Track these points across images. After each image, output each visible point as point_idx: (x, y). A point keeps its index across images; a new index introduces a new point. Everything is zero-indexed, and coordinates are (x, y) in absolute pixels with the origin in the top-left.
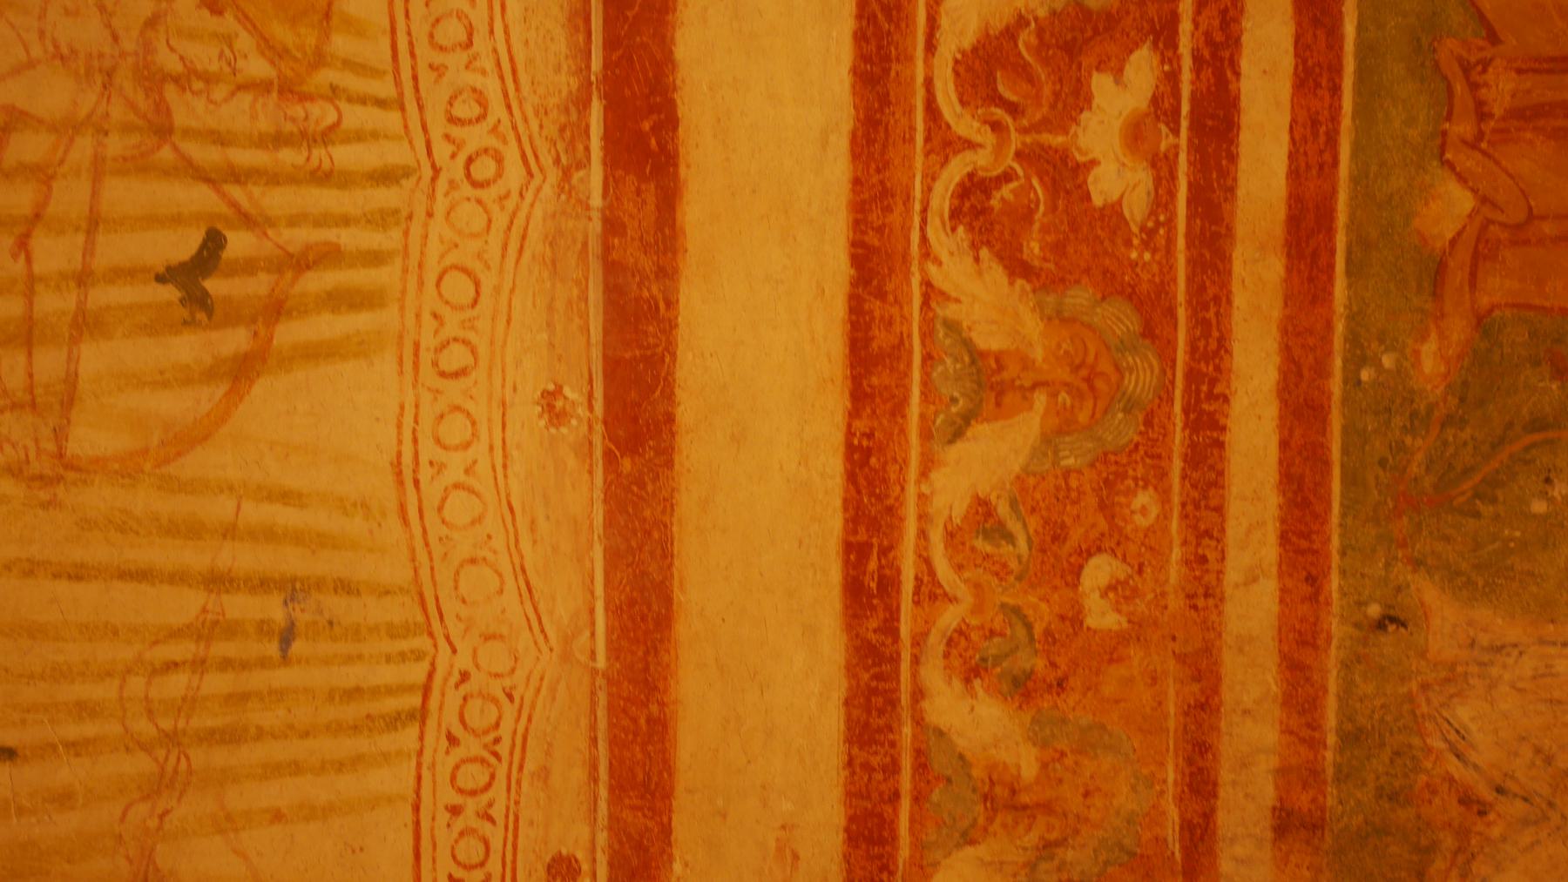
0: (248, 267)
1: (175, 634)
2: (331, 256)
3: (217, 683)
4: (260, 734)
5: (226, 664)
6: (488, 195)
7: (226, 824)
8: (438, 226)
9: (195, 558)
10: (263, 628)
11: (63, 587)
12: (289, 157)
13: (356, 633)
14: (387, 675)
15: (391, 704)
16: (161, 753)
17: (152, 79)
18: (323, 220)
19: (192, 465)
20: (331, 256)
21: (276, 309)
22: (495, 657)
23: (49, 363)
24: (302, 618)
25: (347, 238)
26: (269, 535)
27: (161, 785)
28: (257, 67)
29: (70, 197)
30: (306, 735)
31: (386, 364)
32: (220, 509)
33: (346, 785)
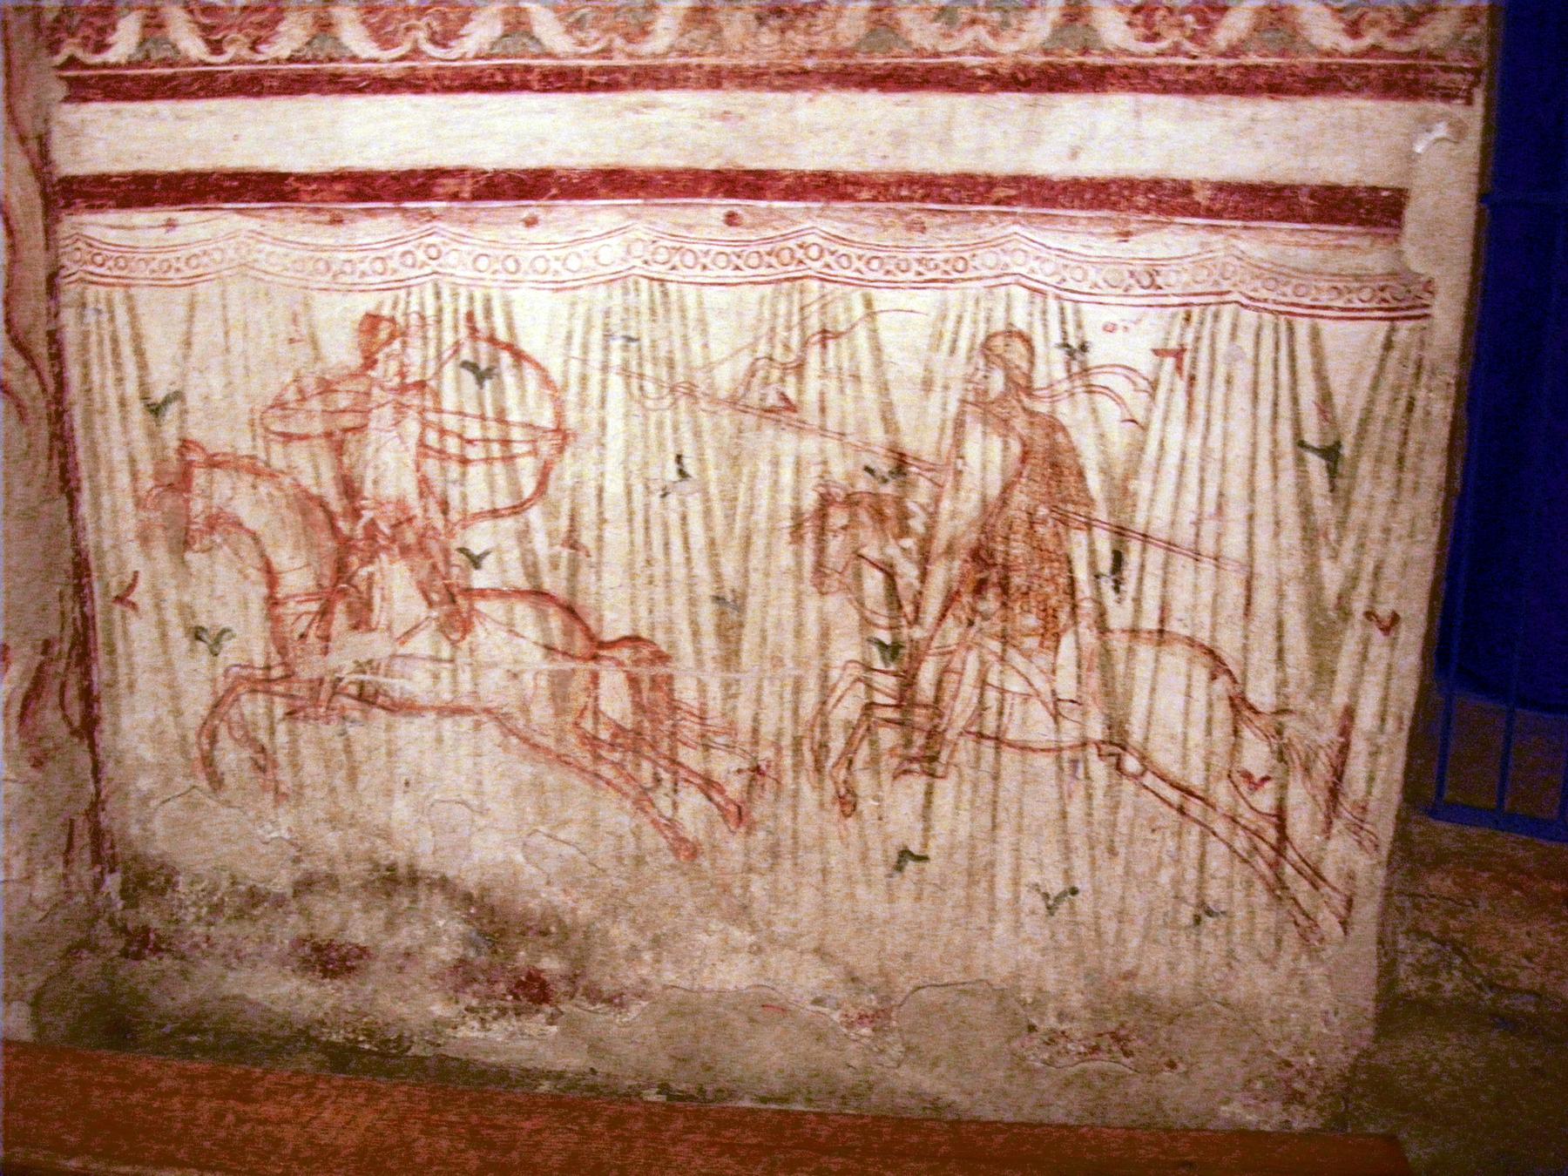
0: (475, 351)
1: (628, 385)
2: (470, 317)
5: (640, 365)
6: (444, 249)
7: (709, 367)
8: (457, 272)
12: (431, 333)
14: (645, 296)
15: (658, 294)
17: (403, 388)
18: (456, 321)
19: (556, 375)
20: (470, 317)
21: (492, 340)
22: (638, 249)
23: (516, 434)
25: (463, 310)
26: (585, 347)
28: (397, 345)
29: (451, 422)
31: (513, 294)
32: (575, 367)
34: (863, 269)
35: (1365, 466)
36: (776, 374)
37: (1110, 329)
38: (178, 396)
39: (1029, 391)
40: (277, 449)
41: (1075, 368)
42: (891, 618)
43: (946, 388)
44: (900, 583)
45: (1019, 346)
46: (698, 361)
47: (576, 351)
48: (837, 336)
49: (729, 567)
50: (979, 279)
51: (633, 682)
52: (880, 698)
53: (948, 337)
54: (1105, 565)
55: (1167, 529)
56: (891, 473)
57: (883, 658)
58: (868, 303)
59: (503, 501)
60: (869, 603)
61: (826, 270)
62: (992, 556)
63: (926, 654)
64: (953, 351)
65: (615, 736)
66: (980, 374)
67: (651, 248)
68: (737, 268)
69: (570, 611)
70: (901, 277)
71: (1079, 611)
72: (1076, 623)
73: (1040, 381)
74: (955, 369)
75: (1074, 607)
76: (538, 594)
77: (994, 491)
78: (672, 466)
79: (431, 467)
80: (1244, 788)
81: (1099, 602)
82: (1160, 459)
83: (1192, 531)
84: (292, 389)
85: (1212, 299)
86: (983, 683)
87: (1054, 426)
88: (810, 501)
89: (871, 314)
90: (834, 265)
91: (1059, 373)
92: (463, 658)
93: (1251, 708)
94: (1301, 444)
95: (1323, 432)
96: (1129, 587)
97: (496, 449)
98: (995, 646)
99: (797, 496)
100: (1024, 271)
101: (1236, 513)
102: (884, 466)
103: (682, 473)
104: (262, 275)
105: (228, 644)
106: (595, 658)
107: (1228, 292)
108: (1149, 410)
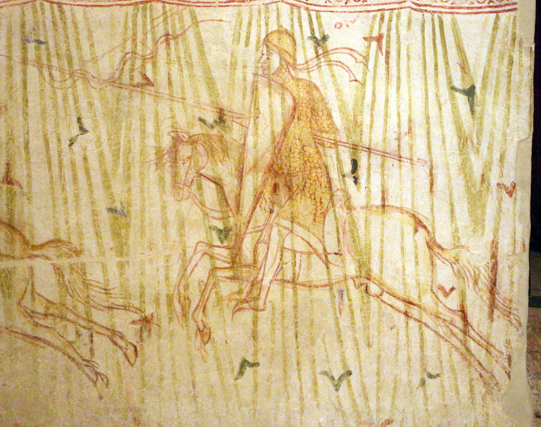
3: (54, 62)
4: (68, 50)
9: (18, 68)
10: (37, 49)
11: (30, 105)
13: (36, 22)
16: (76, 78)
24: (33, 37)
27: (84, 76)
30: (67, 37)
33: (81, 26)
35: (490, 99)
36: (138, 63)
42: (222, 212)
44: (226, 189)
49: (117, 188)
51: (58, 270)
52: (219, 264)
53: (243, 35)
54: (348, 168)
55: (381, 143)
56: (215, 121)
57: (220, 238)
60: (208, 204)
62: (281, 168)
63: (245, 233)
65: (47, 308)
71: (335, 198)
72: (333, 206)
75: (332, 196)
77: (278, 129)
81: (345, 191)
83: (396, 143)
86: (283, 249)
88: (166, 142)
95: (463, 79)
96: (363, 180)
98: (287, 224)
99: (157, 137)
101: (419, 131)
103: (83, 130)
106: (31, 257)
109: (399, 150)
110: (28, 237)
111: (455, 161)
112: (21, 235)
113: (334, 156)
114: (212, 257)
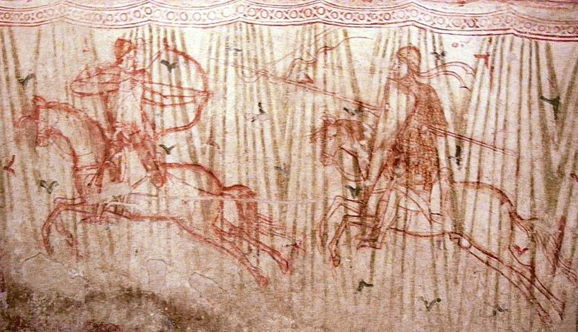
0: (168, 55)
1: (237, 71)
2: (165, 40)
5: (242, 62)
7: (273, 63)
12: (148, 48)
14: (244, 30)
15: (250, 30)
17: (135, 73)
18: (159, 42)
19: (204, 67)
20: (165, 40)
21: (175, 51)
22: (241, 9)
23: (186, 93)
25: (162, 37)
26: (217, 54)
28: (132, 53)
29: (157, 88)
31: (185, 30)
32: (213, 63)
34: (343, 18)
36: (304, 66)
37: (455, 45)
38: (33, 76)
39: (419, 74)
40: (78, 100)
41: (439, 64)
43: (381, 72)
45: (414, 53)
46: (269, 61)
47: (213, 55)
48: (331, 49)
49: (283, 153)
50: (396, 23)
51: (239, 205)
52: (351, 213)
53: (382, 49)
54: (453, 152)
56: (356, 111)
57: (352, 195)
58: (346, 34)
59: (180, 124)
60: (346, 170)
61: (327, 19)
62: (402, 148)
63: (371, 193)
64: (384, 56)
65: (231, 230)
66: (396, 66)
67: (247, 9)
68: (286, 18)
69: (210, 173)
70: (361, 22)
71: (441, 174)
72: (440, 179)
73: (423, 69)
74: (385, 64)
75: (439, 171)
76: (196, 166)
77: (403, 119)
78: (257, 108)
79: (148, 108)
80: (516, 253)
81: (450, 169)
82: (477, 105)
83: (492, 137)
84: (84, 73)
85: (501, 32)
86: (398, 206)
87: (429, 89)
88: (319, 124)
89: (347, 39)
90: (330, 17)
91: (432, 65)
92: (161, 195)
93: (519, 217)
94: (542, 98)
95: (552, 92)
96: (464, 163)
97: (177, 100)
98: (403, 189)
99: (313, 121)
100: (416, 19)
101: (512, 129)
102: (353, 108)
103: (261, 111)
104: (71, 21)
105: (55, 188)
106: (222, 194)
107: (509, 29)
108: (473, 82)
109: (494, 143)
110: (221, 181)
111: (538, 153)
112: (216, 179)
113: (444, 142)
114: (346, 207)
